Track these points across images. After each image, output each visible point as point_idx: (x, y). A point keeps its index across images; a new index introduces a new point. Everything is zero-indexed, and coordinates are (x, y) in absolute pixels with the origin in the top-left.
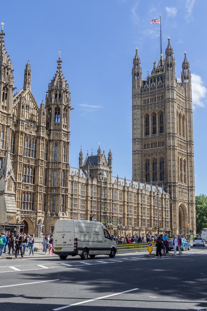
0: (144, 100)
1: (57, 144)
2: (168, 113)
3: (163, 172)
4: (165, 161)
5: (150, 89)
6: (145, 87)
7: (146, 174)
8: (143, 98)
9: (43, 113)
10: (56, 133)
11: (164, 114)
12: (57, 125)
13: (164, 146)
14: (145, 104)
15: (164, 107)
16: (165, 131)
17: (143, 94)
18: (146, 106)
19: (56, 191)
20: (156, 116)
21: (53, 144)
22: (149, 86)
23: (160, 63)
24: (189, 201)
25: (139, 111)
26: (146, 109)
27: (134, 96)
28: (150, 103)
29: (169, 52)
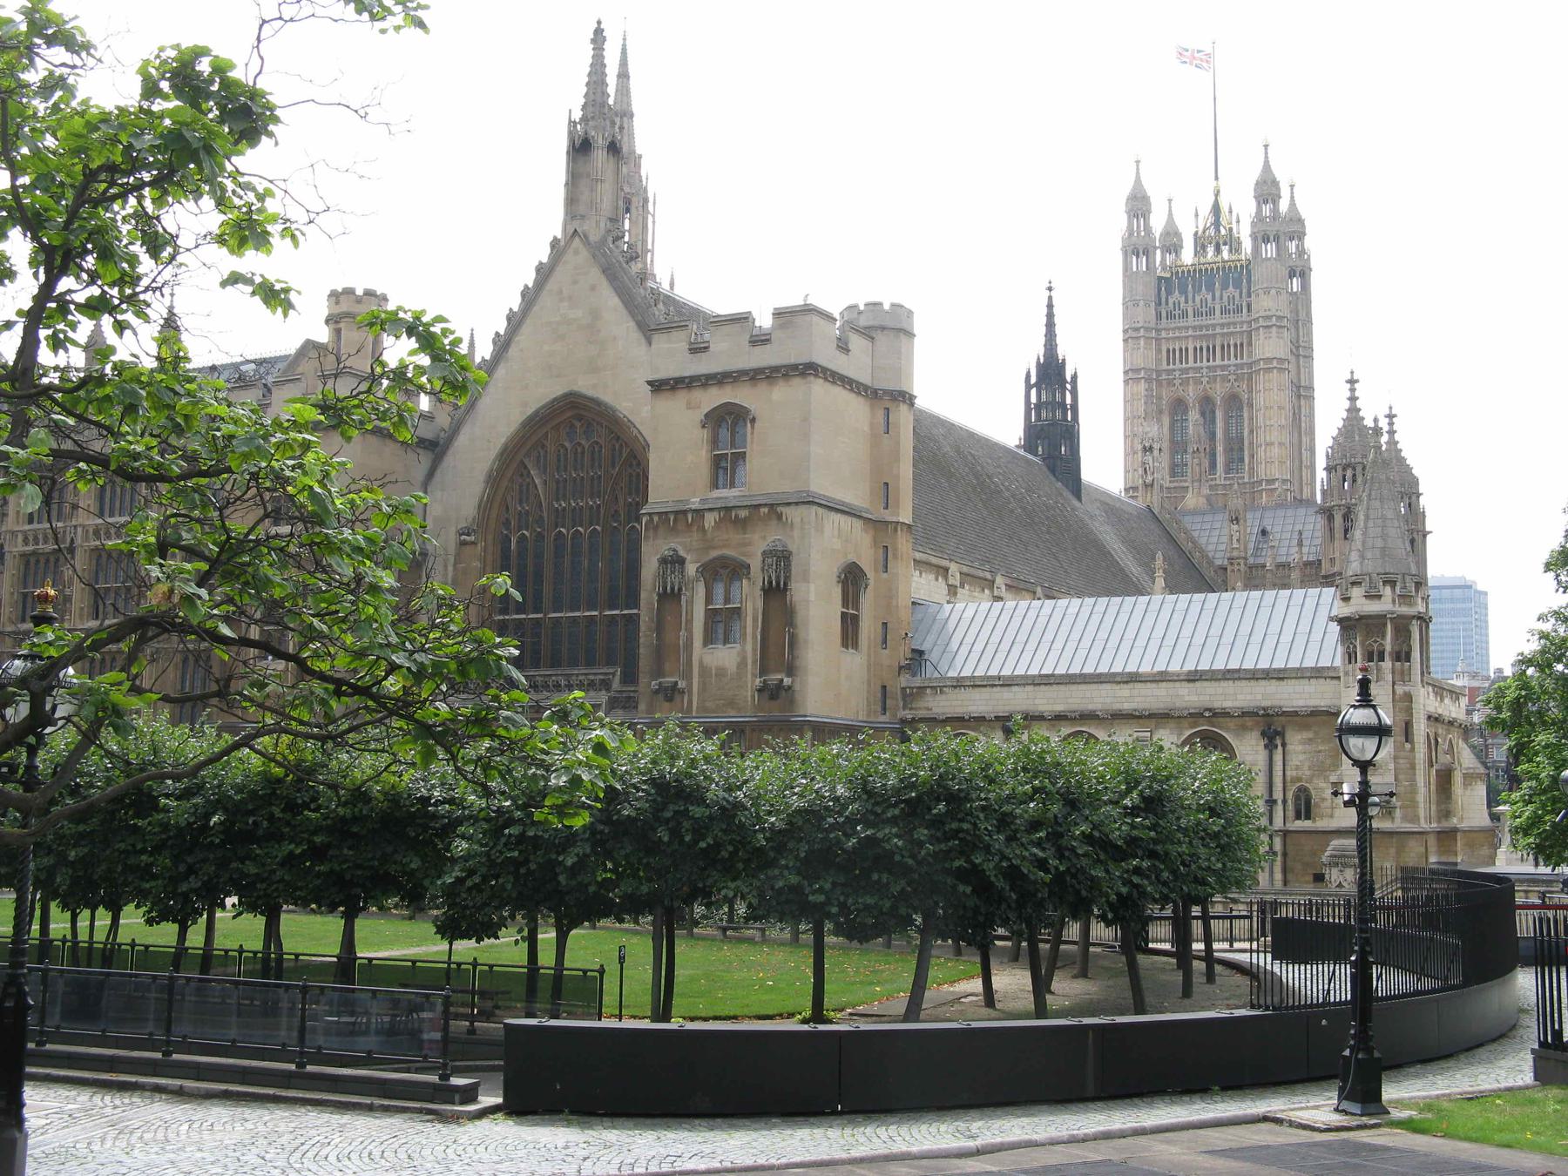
0: (1168, 351)
2: (1266, 408)
6: (1171, 305)
11: (1245, 408)
17: (1167, 330)
18: (1177, 373)
20: (1214, 412)
26: (1177, 382)
28: (1191, 364)
29: (1267, 190)
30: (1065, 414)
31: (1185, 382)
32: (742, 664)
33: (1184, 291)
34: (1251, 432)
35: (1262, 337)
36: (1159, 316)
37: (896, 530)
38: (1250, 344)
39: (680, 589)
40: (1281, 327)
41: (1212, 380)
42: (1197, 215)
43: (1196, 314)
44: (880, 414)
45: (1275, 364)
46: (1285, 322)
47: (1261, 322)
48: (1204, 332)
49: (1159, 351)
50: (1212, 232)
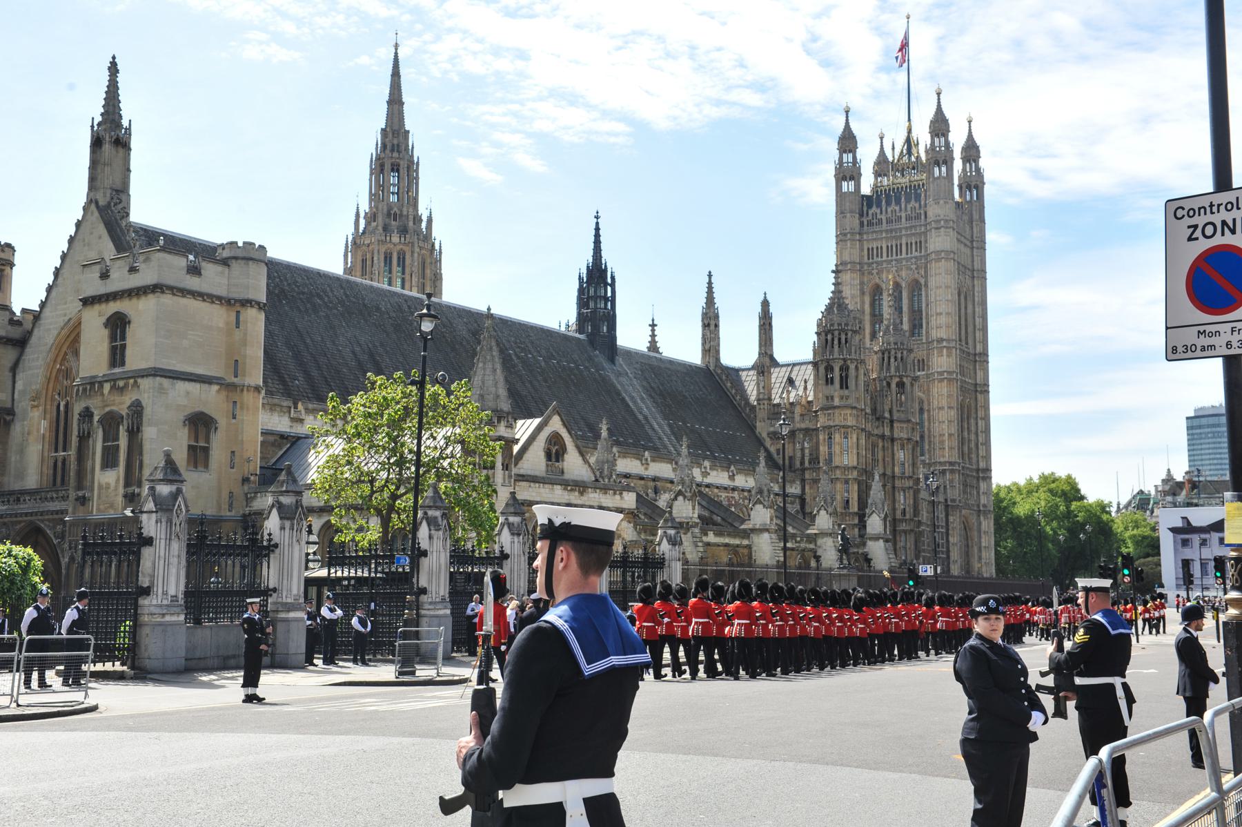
0: (868, 249)
2: (937, 288)
5: (884, 221)
6: (870, 218)
8: (865, 242)
11: (923, 289)
13: (923, 370)
14: (873, 259)
15: (926, 272)
16: (927, 332)
17: (867, 233)
18: (875, 265)
23: (906, 147)
24: (978, 506)
25: (857, 276)
26: (875, 272)
27: (841, 238)
28: (885, 258)
29: (940, 125)
30: (606, 304)
32: (118, 480)
33: (879, 205)
34: (927, 305)
35: (933, 235)
36: (862, 224)
37: (242, 390)
38: (926, 241)
39: (89, 433)
42: (893, 148)
43: (889, 221)
44: (234, 315)
48: (894, 234)
49: (862, 250)
50: (906, 159)
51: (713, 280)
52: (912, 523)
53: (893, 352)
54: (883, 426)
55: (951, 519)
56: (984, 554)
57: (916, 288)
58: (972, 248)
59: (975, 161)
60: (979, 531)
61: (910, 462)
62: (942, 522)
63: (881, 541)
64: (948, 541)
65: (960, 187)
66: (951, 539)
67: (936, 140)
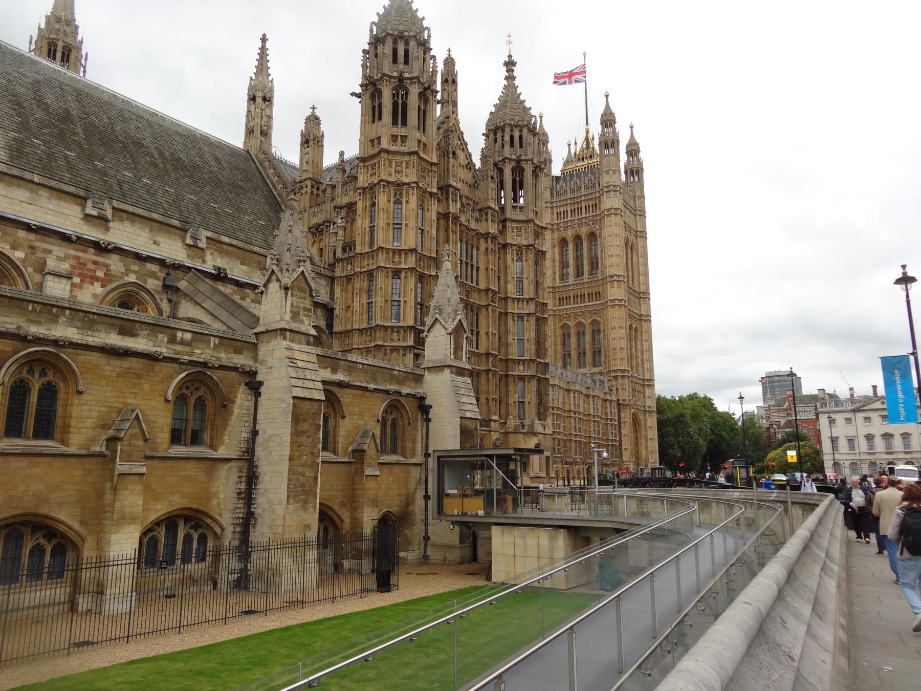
1: (521, 254)
3: (600, 351)
4: (602, 328)
7: (565, 355)
9: (492, 178)
10: (517, 228)
11: (598, 239)
12: (518, 210)
16: (602, 272)
18: (562, 224)
19: (526, 369)
20: (582, 244)
21: (512, 255)
22: (568, 186)
24: (644, 406)
28: (569, 218)
29: (608, 120)
31: (566, 229)
36: (552, 195)
40: (615, 191)
41: (581, 225)
43: (572, 191)
45: (612, 211)
46: (618, 189)
47: (605, 190)
48: (576, 200)
49: (553, 214)
51: (268, 45)
52: (534, 366)
53: (507, 130)
54: (487, 220)
55: (622, 415)
56: (649, 445)
57: (593, 236)
58: (635, 215)
59: (636, 155)
60: (646, 427)
61: (532, 277)
62: (615, 416)
63: (447, 371)
64: (620, 432)
65: (626, 172)
66: (622, 431)
67: (606, 130)
